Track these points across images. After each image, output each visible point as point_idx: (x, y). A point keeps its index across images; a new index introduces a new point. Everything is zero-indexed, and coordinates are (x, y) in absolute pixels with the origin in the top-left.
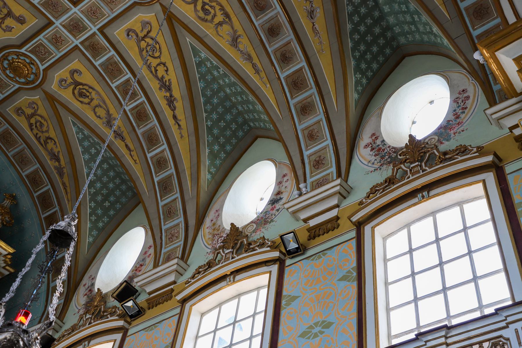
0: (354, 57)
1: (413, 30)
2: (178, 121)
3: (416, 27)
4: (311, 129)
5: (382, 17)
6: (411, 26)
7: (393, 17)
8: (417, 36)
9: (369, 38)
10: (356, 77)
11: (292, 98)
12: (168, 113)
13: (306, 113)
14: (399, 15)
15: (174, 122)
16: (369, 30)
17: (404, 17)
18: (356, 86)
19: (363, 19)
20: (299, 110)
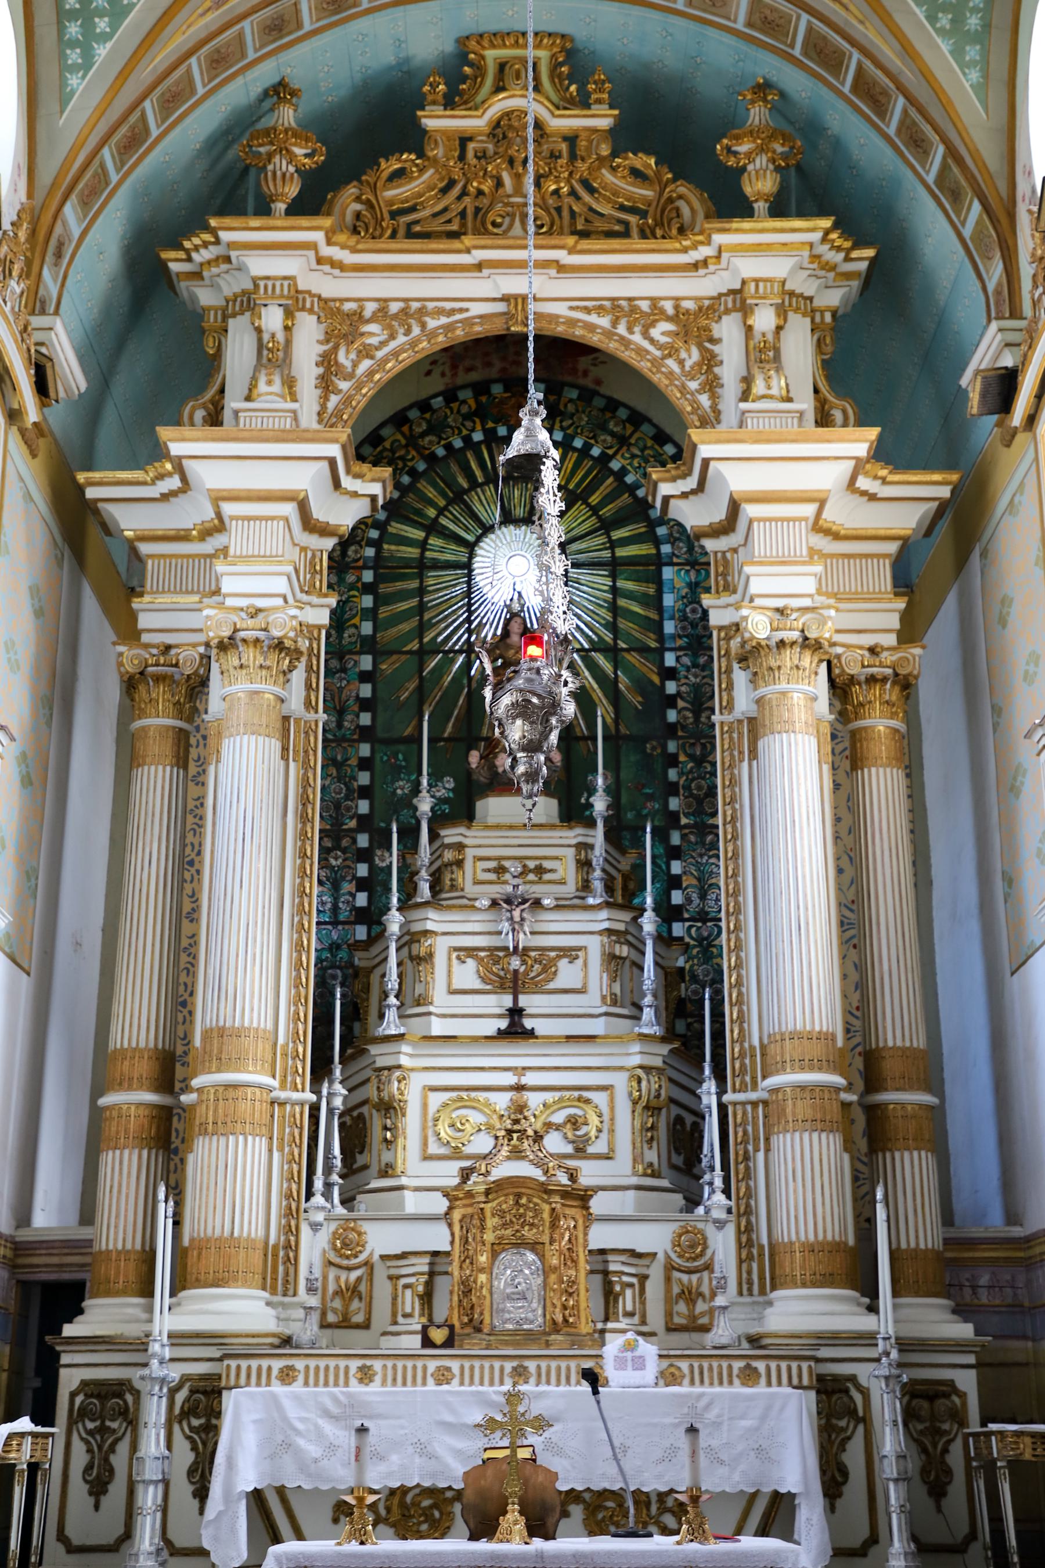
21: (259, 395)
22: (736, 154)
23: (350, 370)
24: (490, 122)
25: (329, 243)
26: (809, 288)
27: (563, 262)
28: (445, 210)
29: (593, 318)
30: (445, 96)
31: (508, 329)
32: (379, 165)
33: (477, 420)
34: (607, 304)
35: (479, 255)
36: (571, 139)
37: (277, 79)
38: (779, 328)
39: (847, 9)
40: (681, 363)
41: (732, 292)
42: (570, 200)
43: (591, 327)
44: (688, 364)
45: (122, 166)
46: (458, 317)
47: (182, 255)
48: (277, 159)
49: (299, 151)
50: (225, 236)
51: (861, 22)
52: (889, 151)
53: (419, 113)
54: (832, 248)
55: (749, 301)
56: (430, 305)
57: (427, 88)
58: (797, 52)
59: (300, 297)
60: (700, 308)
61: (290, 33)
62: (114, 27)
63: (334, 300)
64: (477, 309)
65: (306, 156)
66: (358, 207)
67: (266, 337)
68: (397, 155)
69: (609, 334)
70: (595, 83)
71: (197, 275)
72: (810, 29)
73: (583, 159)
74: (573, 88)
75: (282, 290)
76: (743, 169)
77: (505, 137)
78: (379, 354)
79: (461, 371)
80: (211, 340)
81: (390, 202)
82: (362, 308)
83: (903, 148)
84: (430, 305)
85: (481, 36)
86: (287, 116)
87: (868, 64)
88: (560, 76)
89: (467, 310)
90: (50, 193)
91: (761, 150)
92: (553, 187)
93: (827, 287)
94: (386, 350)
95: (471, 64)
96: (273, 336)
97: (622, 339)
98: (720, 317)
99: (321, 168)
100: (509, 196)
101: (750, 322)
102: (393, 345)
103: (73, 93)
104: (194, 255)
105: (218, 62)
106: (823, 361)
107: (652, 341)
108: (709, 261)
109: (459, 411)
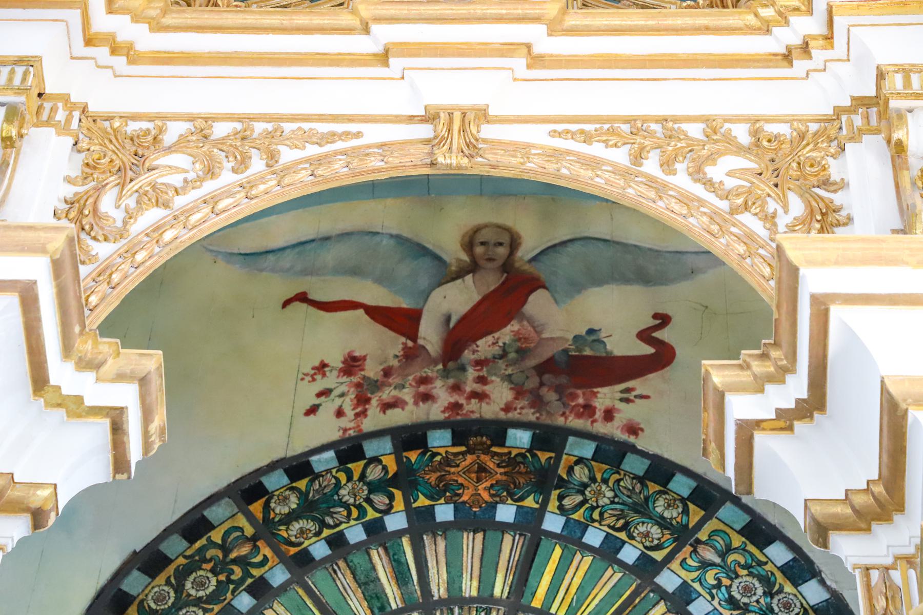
23: (119, 224)
27: (537, 50)
29: (597, 150)
31: (433, 164)
33: (398, 494)
34: (625, 128)
40: (770, 219)
43: (594, 163)
44: (783, 221)
60: (802, 136)
64: (374, 134)
69: (626, 174)
79: (373, 408)
84: (288, 127)
94: (193, 195)
97: (651, 182)
102: (210, 186)
107: (709, 184)
109: (362, 477)
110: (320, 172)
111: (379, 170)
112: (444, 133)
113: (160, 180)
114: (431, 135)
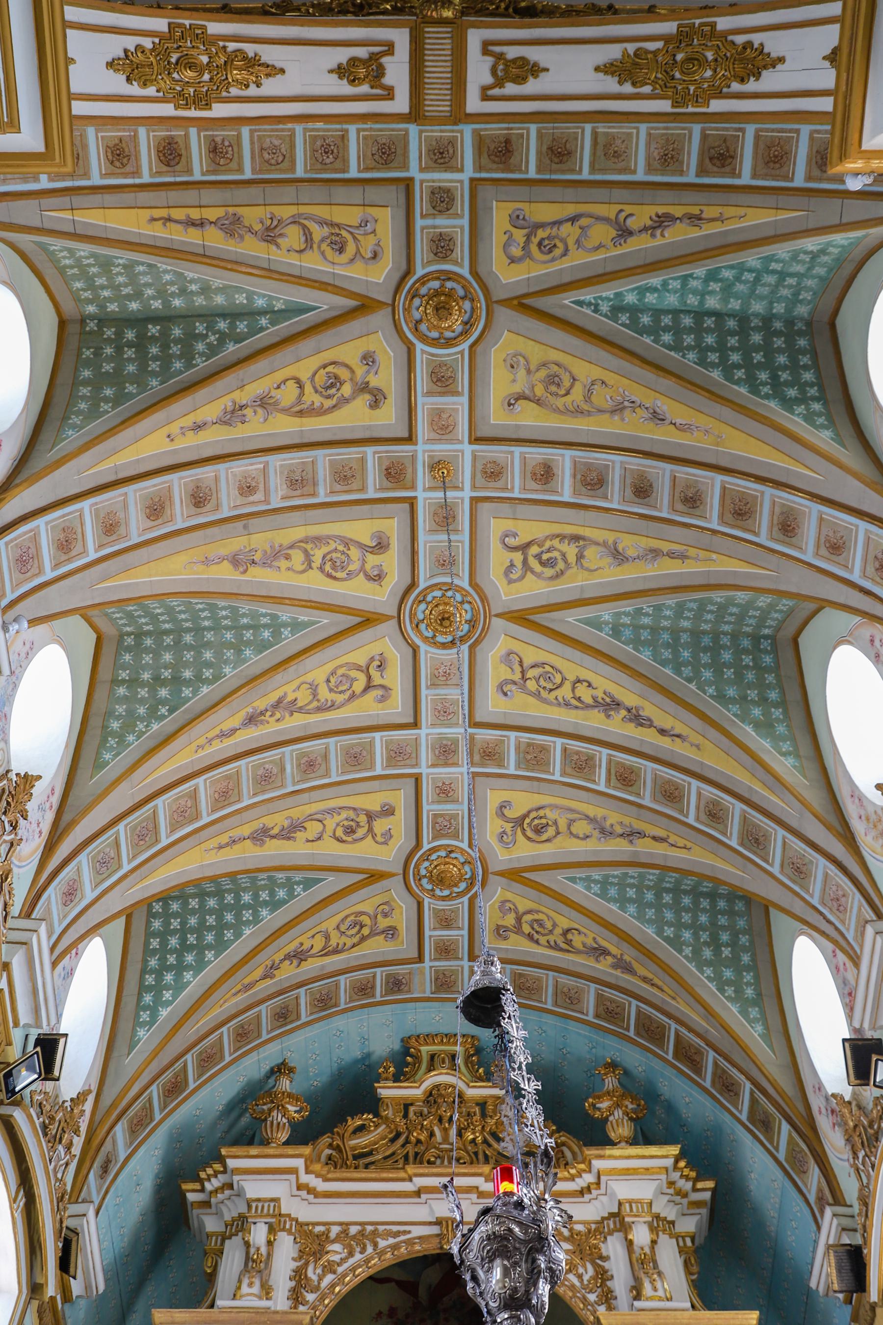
0: (767, 397)
1: (794, 283)
2: (672, 733)
3: (792, 275)
4: (823, 539)
5: (743, 319)
6: (786, 283)
7: (754, 302)
8: (810, 283)
9: (758, 357)
10: (799, 415)
11: (756, 534)
12: (648, 737)
13: (794, 528)
14: (757, 292)
15: (667, 740)
16: (746, 349)
17: (764, 285)
18: (812, 423)
19: (722, 348)
20: (782, 537)
21: (241, 1296)
22: (599, 1109)
24: (425, 1092)
25: (307, 1172)
26: (670, 1213)
28: (393, 1154)
30: (394, 1075)
31: (442, 1248)
32: (347, 1121)
35: (420, 1182)
36: (482, 1104)
37: (281, 1061)
38: (654, 1242)
39: (663, 991)
41: (612, 1215)
42: (485, 1146)
45: (165, 1107)
46: (402, 1238)
47: (197, 1186)
48: (275, 1113)
49: (291, 1108)
50: (231, 1163)
51: (674, 998)
52: (708, 1102)
53: (376, 1085)
54: (682, 1176)
55: (627, 1219)
56: (381, 1228)
57: (382, 1070)
58: (632, 1034)
59: (282, 1220)
60: (589, 1231)
61: (292, 1022)
62: (175, 997)
63: (308, 1224)
65: (295, 1112)
66: (328, 1152)
67: (252, 1250)
68: (359, 1115)
70: (496, 1066)
71: (206, 1204)
72: (639, 1012)
73: (491, 1117)
74: (481, 1070)
75: (269, 1210)
76: (606, 1119)
77: (435, 1102)
78: (340, 1270)
80: (210, 1259)
81: (354, 1148)
82: (329, 1231)
83: (718, 1096)
85: (418, 1036)
86: (285, 1084)
87: (683, 1030)
88: (472, 1062)
89: (409, 1232)
90: (108, 1112)
91: (618, 1105)
92: (471, 1137)
93: (683, 1215)
95: (411, 1056)
96: (258, 1249)
98: (605, 1238)
99: (307, 1121)
100: (440, 1144)
101: (630, 1237)
102: (351, 1261)
103: (139, 1040)
104: (207, 1185)
105: (243, 1036)
106: (692, 1281)
108: (592, 1187)
110: (396, 1253)
111: (419, 1251)
112: (445, 1232)
113: (331, 1259)
114: (439, 1232)
